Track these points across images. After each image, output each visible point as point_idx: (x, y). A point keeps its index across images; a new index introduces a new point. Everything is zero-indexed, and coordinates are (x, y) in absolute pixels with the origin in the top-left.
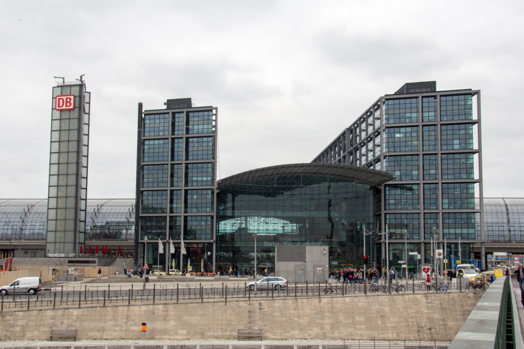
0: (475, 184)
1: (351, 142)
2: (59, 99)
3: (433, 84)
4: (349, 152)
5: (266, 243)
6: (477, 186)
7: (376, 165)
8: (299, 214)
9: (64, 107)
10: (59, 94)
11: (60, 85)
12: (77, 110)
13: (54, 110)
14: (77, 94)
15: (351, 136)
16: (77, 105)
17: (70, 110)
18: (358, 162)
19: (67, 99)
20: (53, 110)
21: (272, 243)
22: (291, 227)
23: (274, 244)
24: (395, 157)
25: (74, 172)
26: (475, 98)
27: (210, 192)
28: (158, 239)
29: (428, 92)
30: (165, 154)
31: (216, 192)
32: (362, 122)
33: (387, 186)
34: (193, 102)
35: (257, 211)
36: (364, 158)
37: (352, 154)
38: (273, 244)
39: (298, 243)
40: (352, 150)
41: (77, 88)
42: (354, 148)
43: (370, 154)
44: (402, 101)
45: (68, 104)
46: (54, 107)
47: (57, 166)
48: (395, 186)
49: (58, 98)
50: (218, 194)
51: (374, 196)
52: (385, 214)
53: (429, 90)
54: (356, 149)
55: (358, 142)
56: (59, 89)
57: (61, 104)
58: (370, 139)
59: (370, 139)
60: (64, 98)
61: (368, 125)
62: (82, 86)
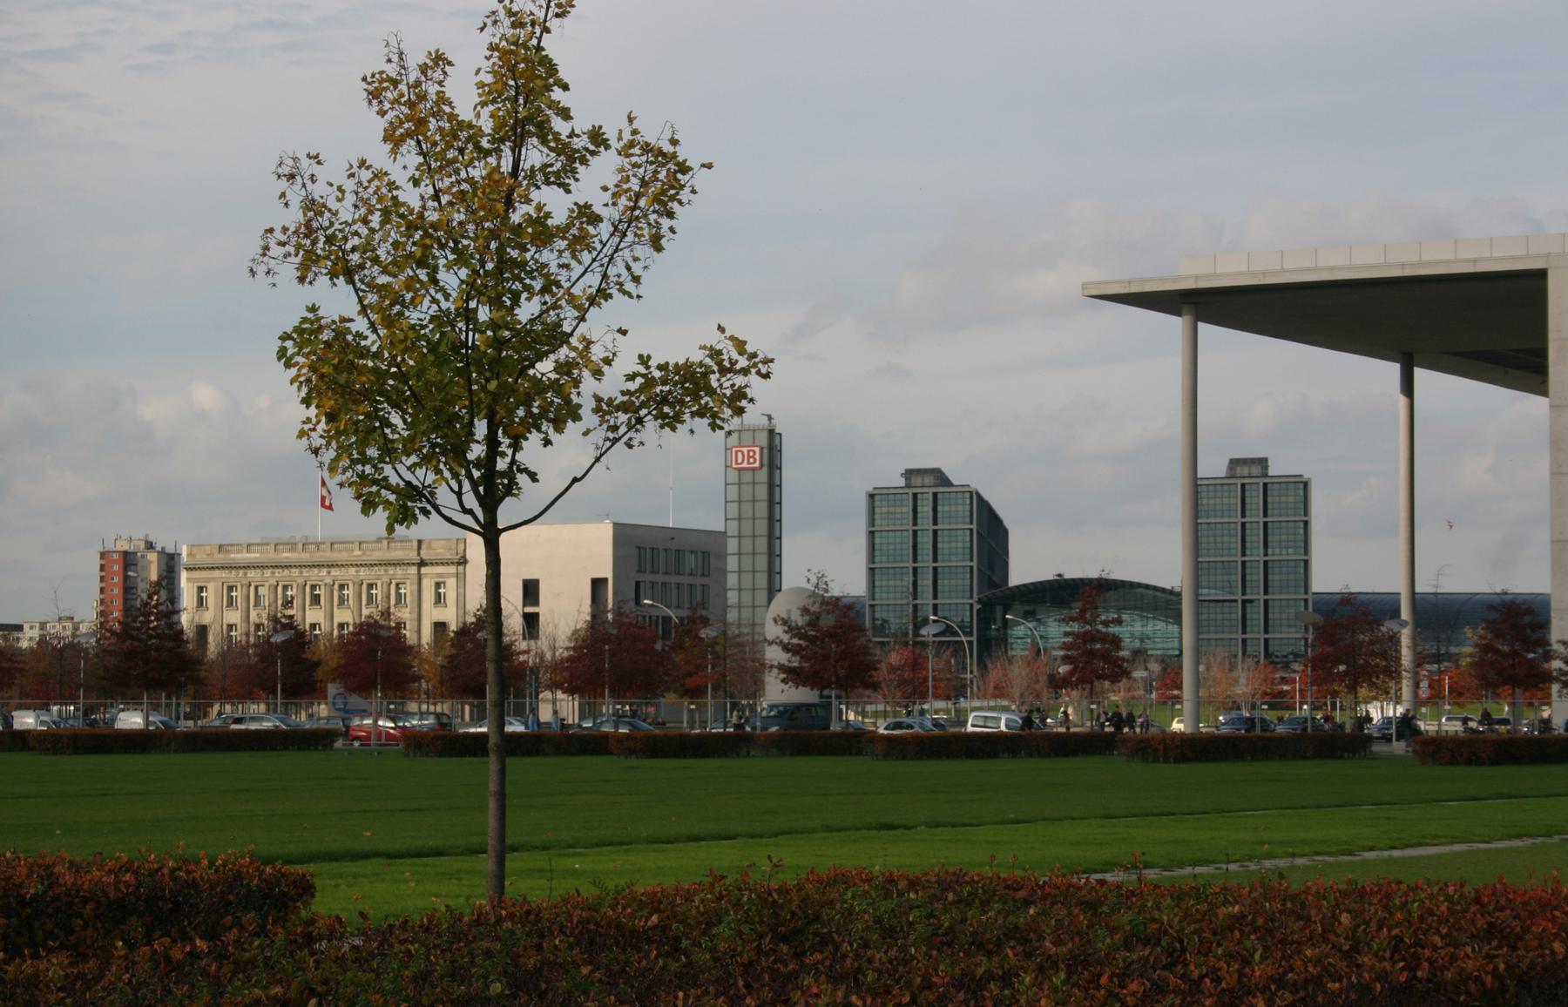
2: (737, 452)
3: (1263, 462)
9: (745, 465)
12: (765, 469)
13: (729, 469)
14: (765, 443)
16: (766, 461)
17: (754, 469)
19: (749, 451)
30: (905, 552)
31: (976, 607)
41: (765, 434)
44: (1226, 488)
46: (728, 464)
47: (736, 557)
50: (978, 610)
57: (740, 460)
60: (745, 450)
62: (771, 432)
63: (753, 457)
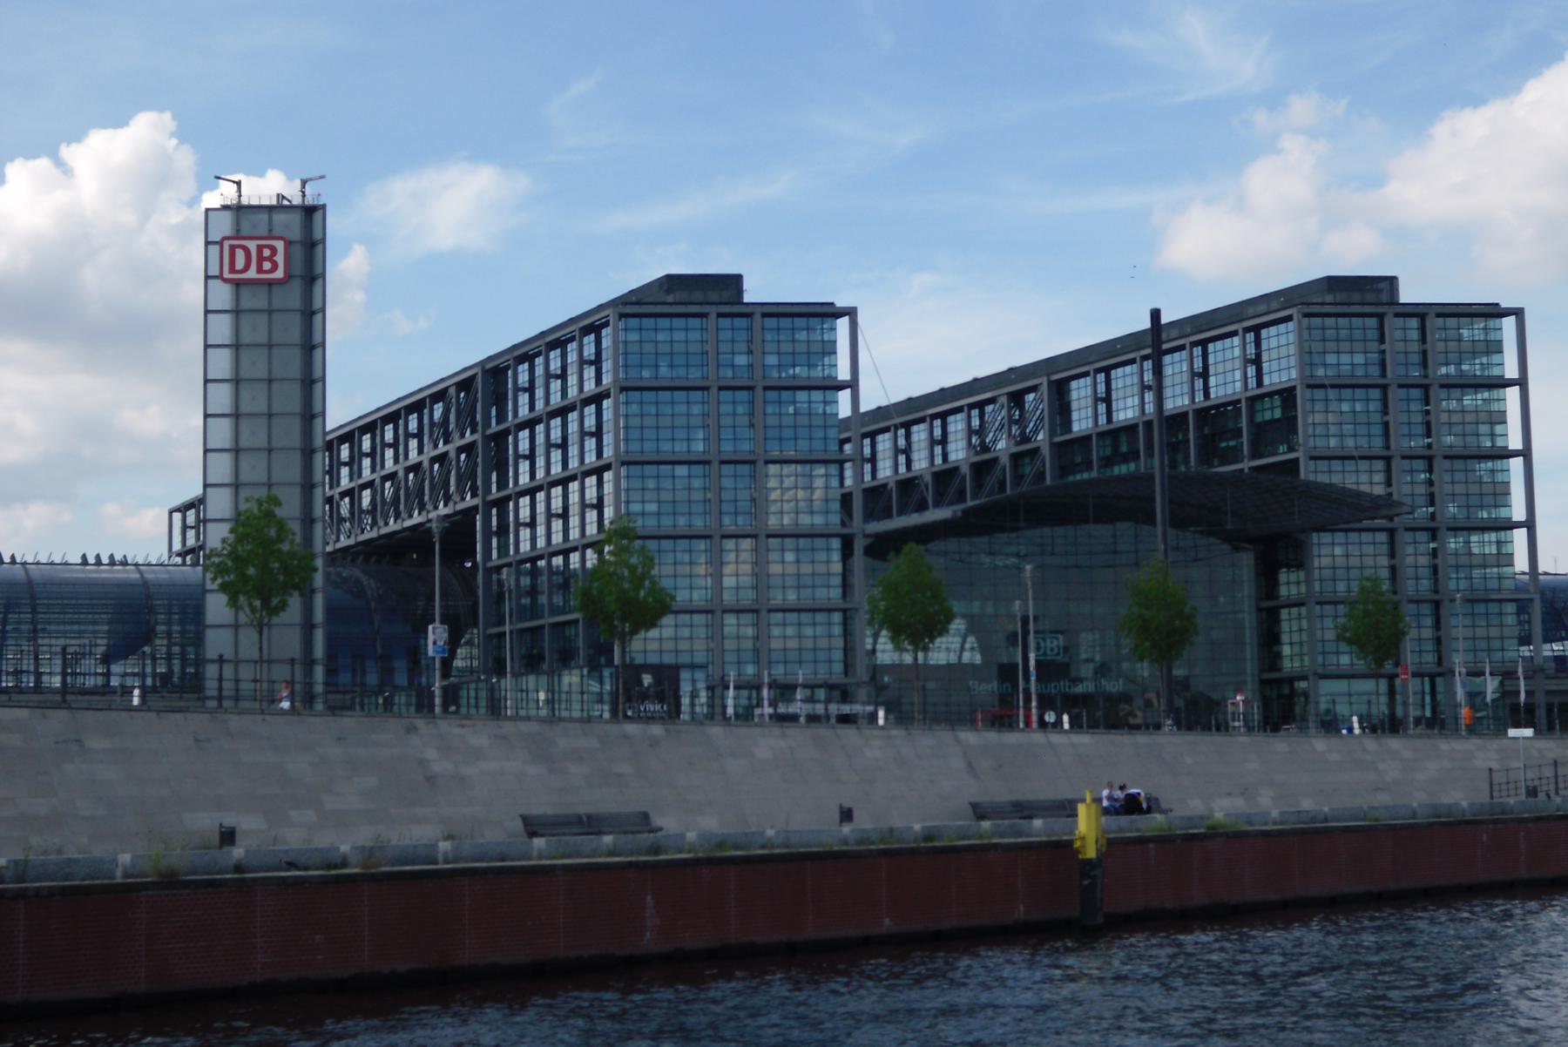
2: (233, 249)
6: (1520, 536)
9: (252, 273)
10: (228, 233)
12: (296, 287)
14: (295, 233)
16: (298, 268)
17: (270, 283)
19: (260, 248)
20: (210, 282)
26: (1509, 323)
27: (836, 543)
34: (746, 285)
39: (1062, 683)
41: (296, 219)
45: (267, 265)
56: (228, 215)
57: (240, 264)
60: (252, 245)
62: (311, 213)
63: (270, 259)
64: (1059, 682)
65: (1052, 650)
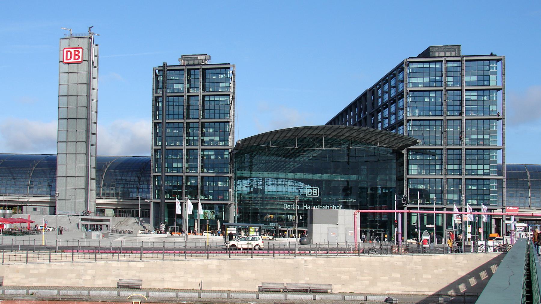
0: (498, 151)
1: (372, 103)
2: (67, 52)
4: (370, 114)
5: (285, 205)
7: (399, 128)
8: (317, 176)
9: (72, 60)
10: (68, 47)
11: (68, 37)
12: (85, 63)
14: (86, 46)
15: (372, 97)
16: (85, 58)
17: (78, 63)
18: (380, 125)
19: (75, 51)
21: (291, 206)
22: (311, 191)
23: (294, 206)
24: (419, 121)
25: (84, 128)
28: (175, 199)
29: (453, 57)
32: (385, 84)
33: (410, 150)
35: (276, 173)
36: (386, 121)
37: (373, 116)
38: (292, 206)
39: (318, 206)
40: (374, 112)
42: (376, 110)
43: (393, 117)
45: (77, 57)
48: (419, 151)
49: (65, 50)
51: (397, 160)
52: (408, 179)
53: (453, 54)
54: (379, 111)
55: (380, 104)
56: (67, 40)
57: (69, 58)
58: (393, 101)
59: (393, 101)
60: (72, 50)
61: (390, 87)
63: (77, 55)
64: (317, 206)
65: (315, 193)
